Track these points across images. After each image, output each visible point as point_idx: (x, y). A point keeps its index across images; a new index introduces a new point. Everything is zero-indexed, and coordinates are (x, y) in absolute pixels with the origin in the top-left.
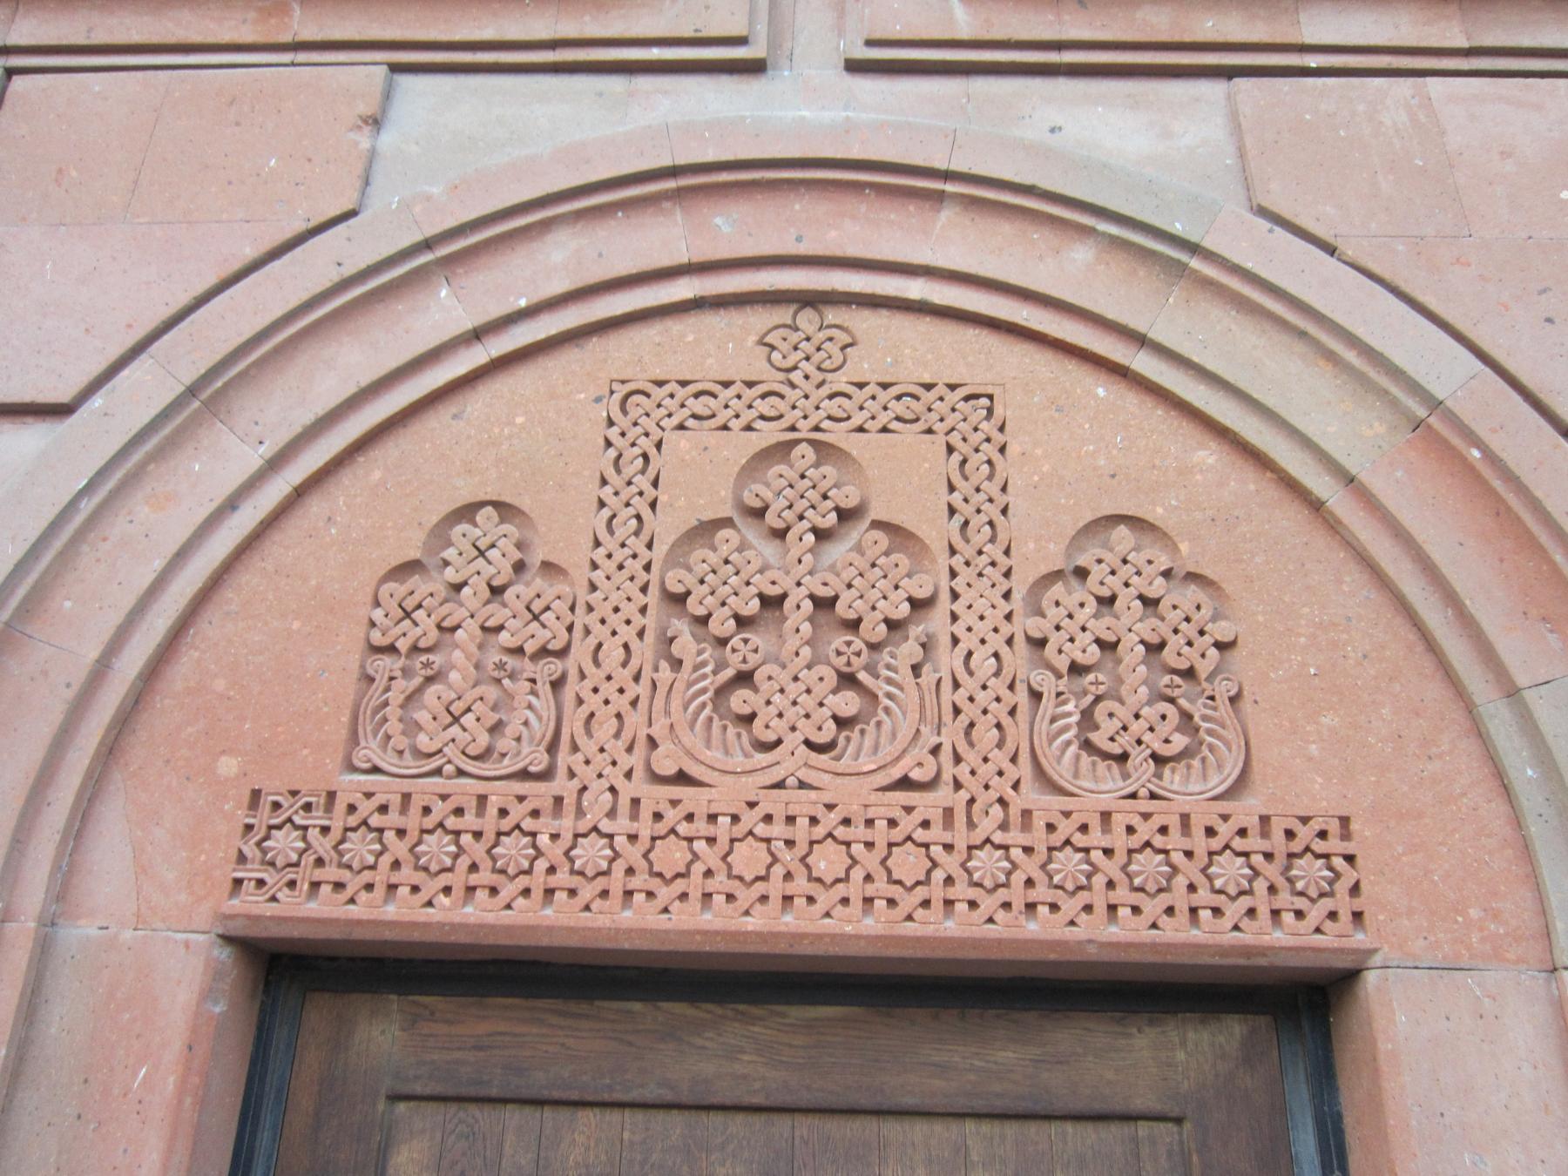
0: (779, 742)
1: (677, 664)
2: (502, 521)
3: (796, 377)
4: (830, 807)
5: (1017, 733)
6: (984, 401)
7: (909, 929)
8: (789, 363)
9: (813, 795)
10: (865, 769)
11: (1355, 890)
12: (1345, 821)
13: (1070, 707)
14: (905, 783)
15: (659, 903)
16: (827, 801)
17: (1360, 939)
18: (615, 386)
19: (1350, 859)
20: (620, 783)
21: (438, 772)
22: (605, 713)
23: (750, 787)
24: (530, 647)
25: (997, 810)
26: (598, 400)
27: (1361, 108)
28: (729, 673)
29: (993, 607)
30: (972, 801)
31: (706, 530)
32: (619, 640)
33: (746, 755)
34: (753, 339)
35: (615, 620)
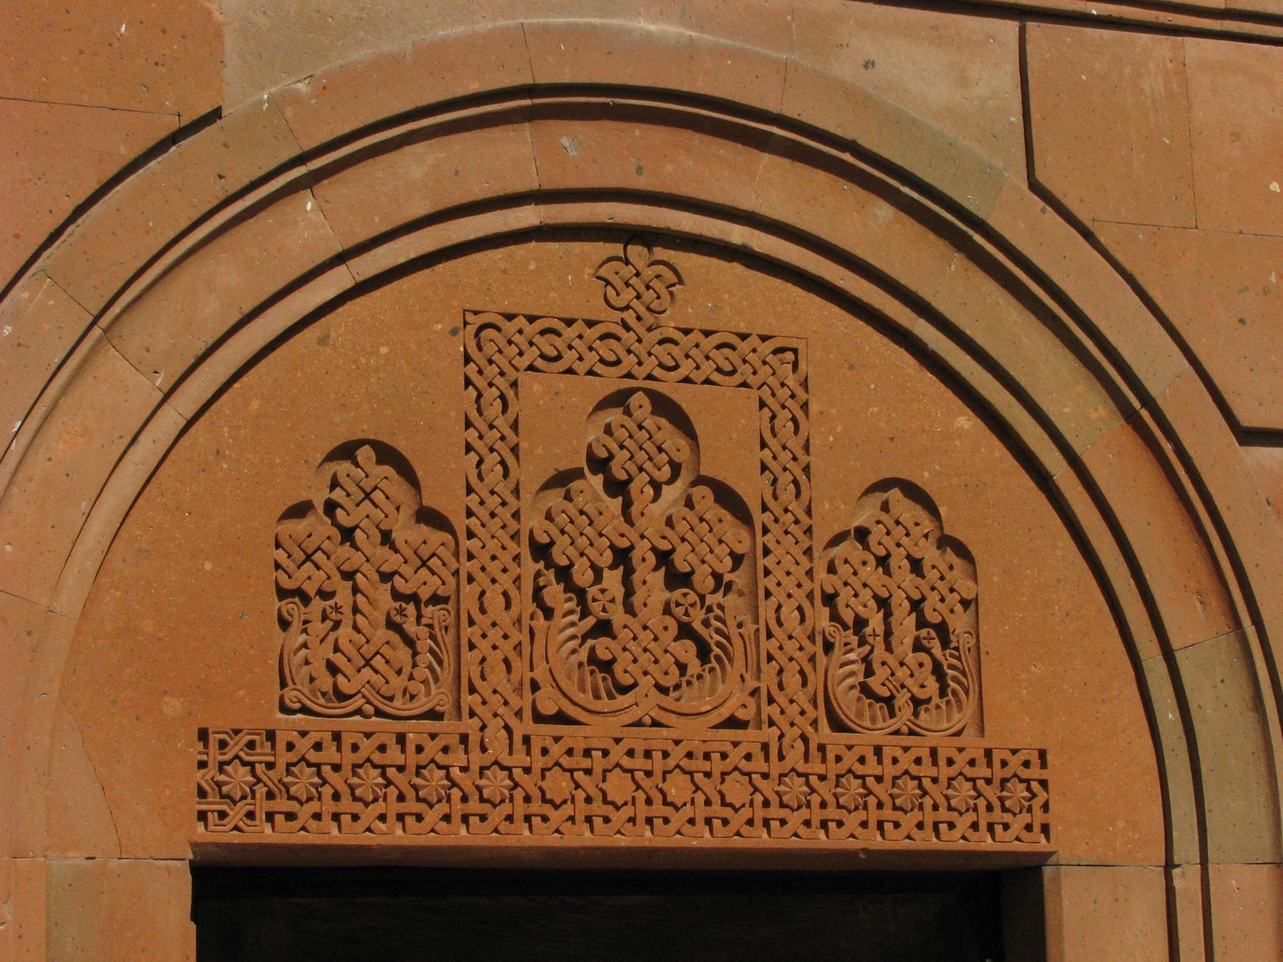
0: (635, 685)
1: (548, 613)
2: (380, 462)
3: (629, 317)
4: (677, 742)
5: (815, 680)
6: (790, 356)
7: (737, 842)
8: (620, 303)
9: (664, 732)
10: (703, 710)
11: (1045, 807)
12: (1042, 754)
13: (852, 656)
14: (733, 723)
15: (552, 824)
16: (675, 737)
17: (1042, 844)
18: (470, 318)
19: (1044, 783)
20: (513, 722)
21: (358, 712)
22: (495, 658)
23: (614, 725)
24: (425, 594)
25: (799, 744)
26: (454, 332)
27: (1128, 70)
28: (591, 621)
29: (797, 563)
30: (781, 736)
31: (562, 480)
32: (498, 588)
33: (611, 697)
34: (589, 271)
35: (494, 568)
